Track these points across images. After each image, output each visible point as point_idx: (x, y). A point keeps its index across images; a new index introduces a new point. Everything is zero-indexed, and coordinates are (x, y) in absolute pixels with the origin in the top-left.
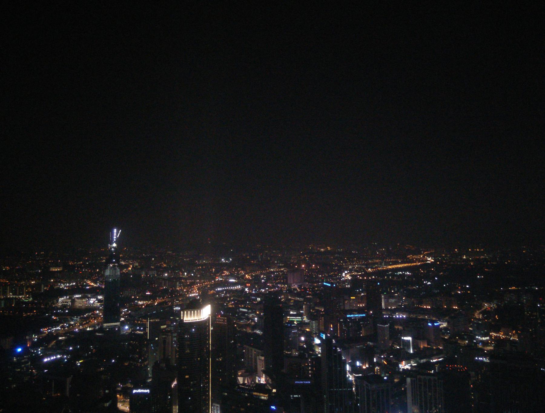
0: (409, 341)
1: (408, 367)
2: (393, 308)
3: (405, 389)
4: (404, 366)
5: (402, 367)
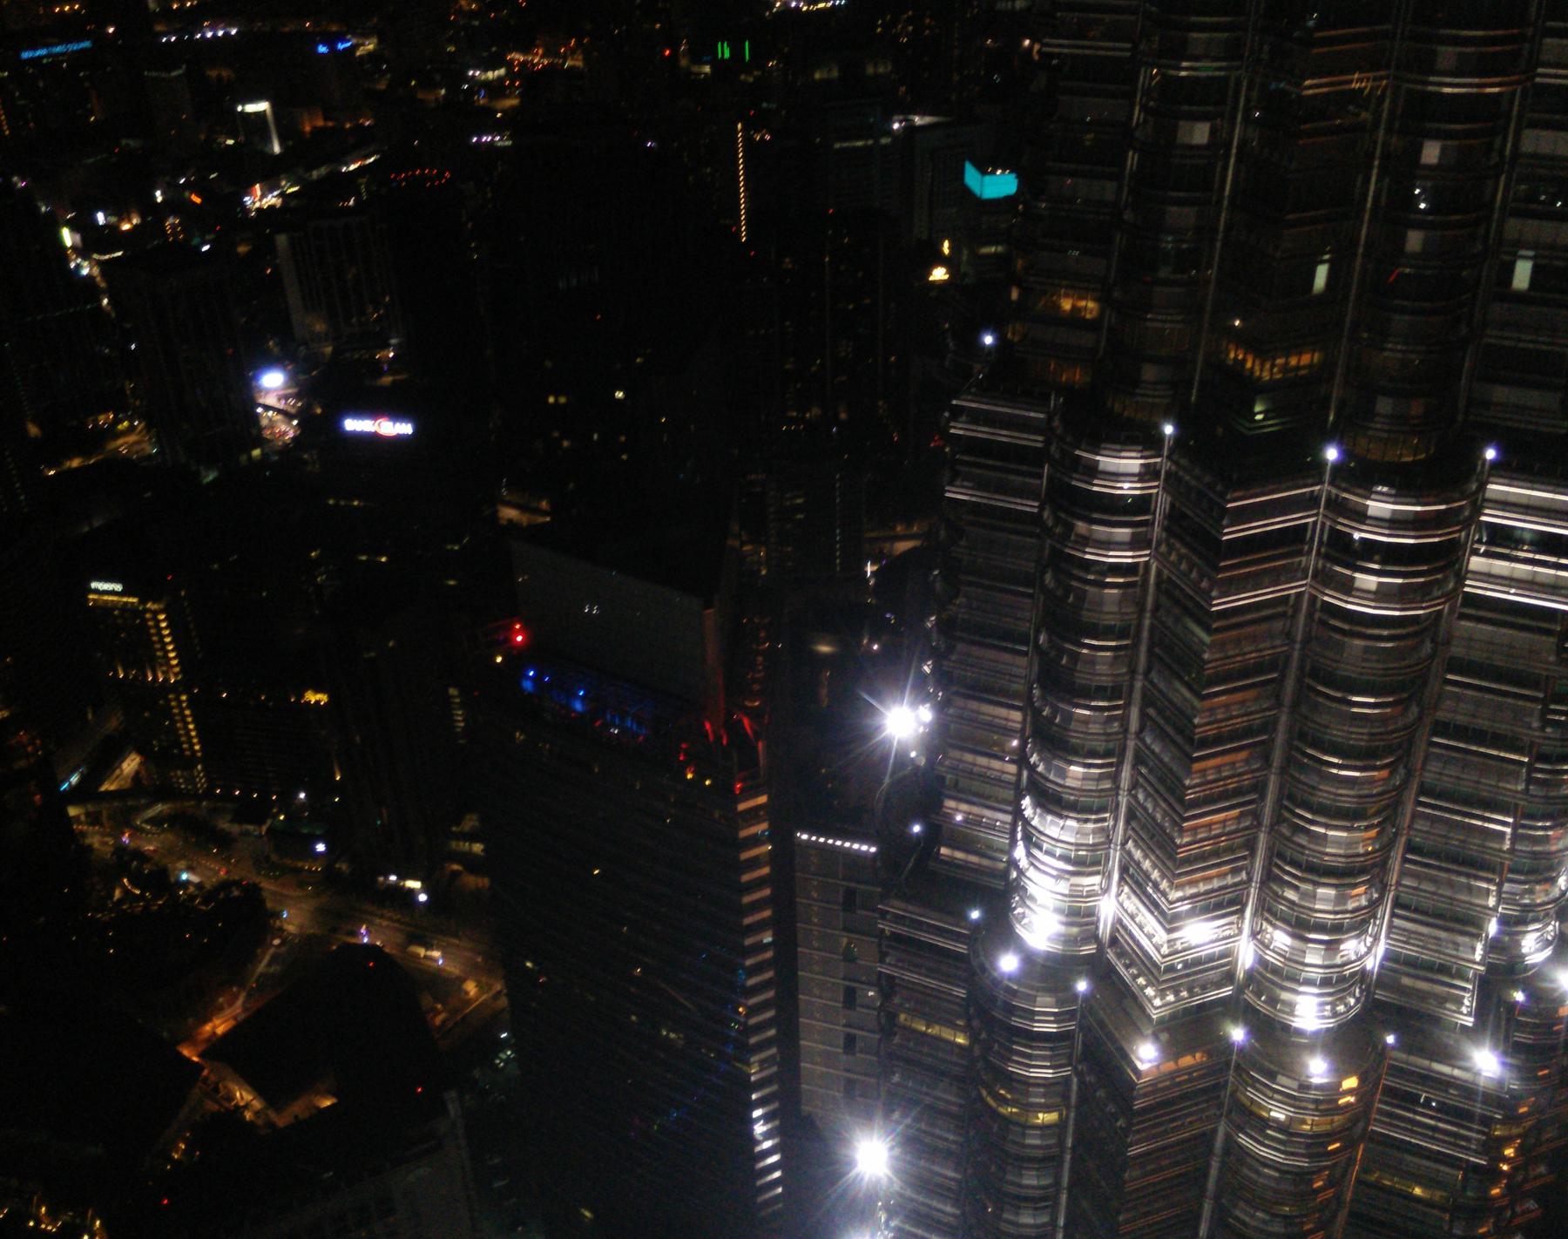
0: (260, 116)
1: (272, 200)
2: (189, 4)
3: (276, 269)
4: (260, 199)
5: (254, 203)
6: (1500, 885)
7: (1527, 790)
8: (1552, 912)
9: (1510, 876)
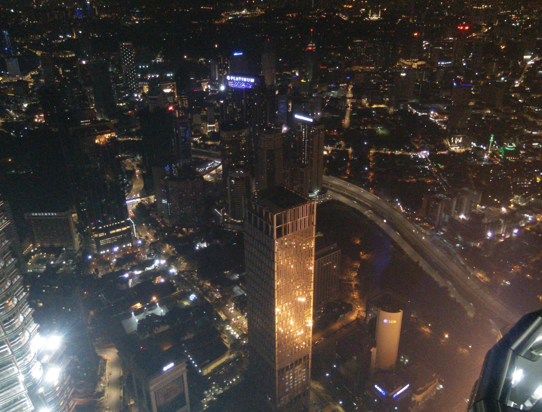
6: (16, 364)
7: (6, 334)
8: (35, 360)
9: (17, 360)
